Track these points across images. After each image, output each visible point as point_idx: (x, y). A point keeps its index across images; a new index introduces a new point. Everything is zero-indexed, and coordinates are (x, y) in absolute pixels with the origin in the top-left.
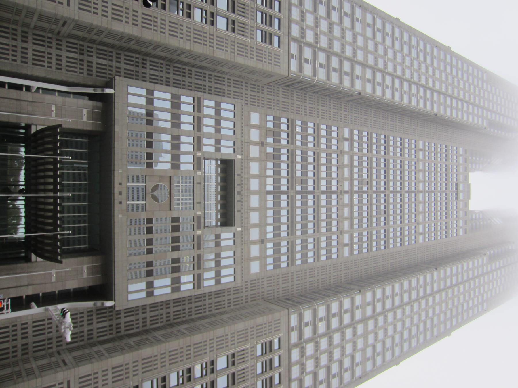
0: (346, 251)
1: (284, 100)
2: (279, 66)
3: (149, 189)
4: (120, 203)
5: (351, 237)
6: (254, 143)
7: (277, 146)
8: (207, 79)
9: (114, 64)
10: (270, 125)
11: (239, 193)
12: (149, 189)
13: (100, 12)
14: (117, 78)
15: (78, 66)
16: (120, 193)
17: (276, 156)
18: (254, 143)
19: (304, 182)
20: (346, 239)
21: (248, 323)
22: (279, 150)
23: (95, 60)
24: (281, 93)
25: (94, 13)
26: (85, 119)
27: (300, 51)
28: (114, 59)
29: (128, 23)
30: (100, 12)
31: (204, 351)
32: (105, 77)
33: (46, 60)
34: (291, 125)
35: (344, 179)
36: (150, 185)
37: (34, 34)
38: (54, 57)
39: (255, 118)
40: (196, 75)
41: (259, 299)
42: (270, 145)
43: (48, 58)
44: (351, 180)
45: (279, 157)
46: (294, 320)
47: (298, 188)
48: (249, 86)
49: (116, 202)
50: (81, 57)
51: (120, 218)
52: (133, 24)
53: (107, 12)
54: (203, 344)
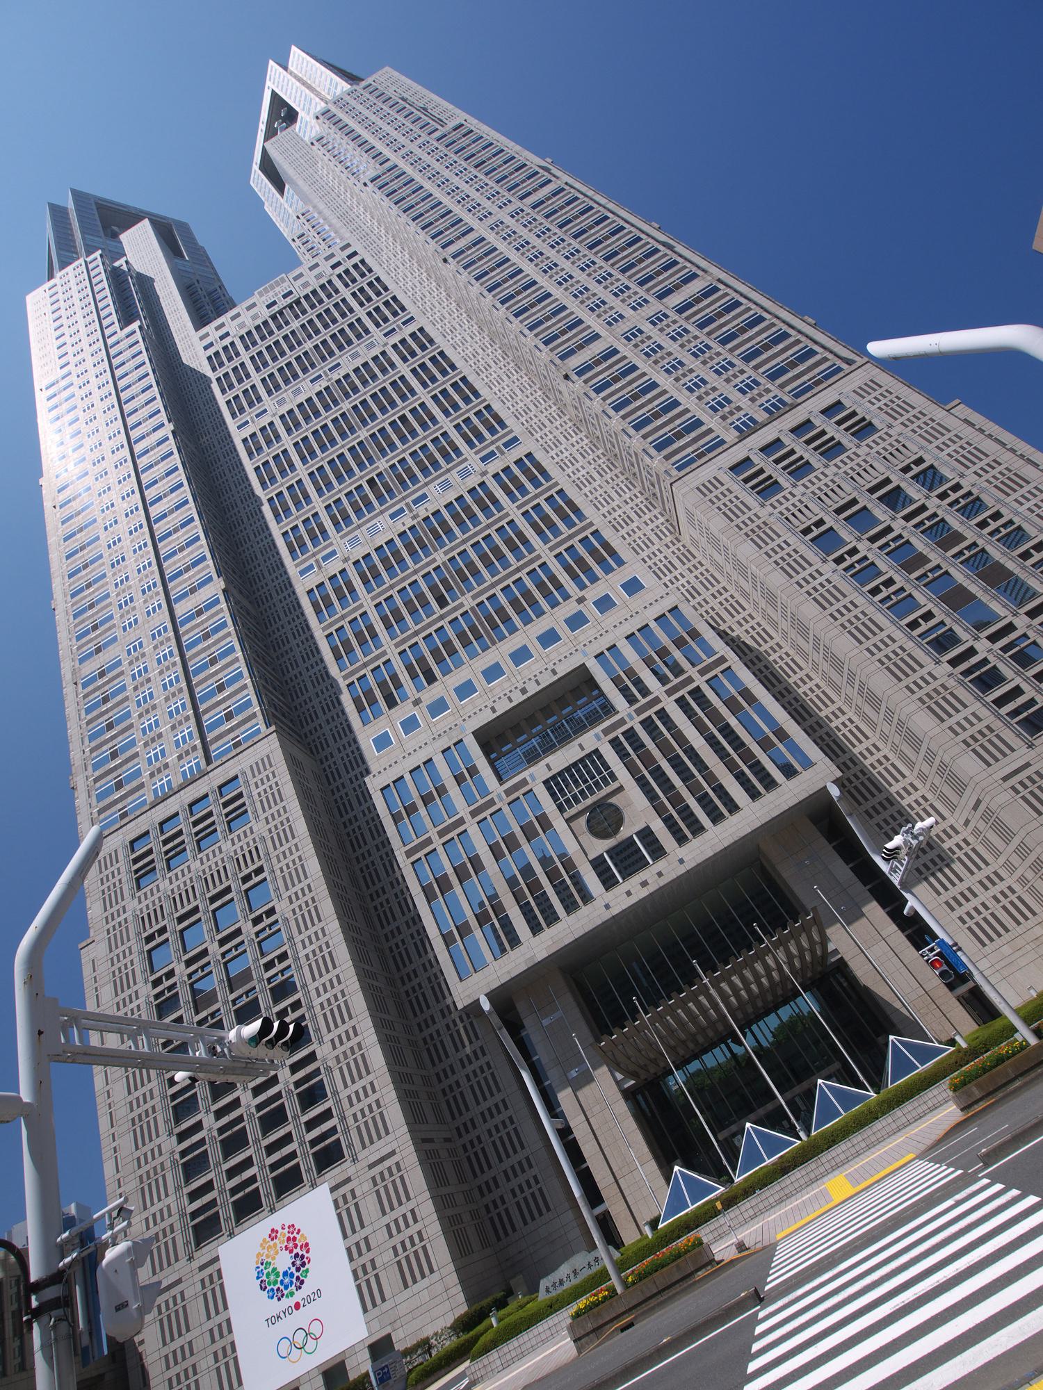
1: (331, 741)
2: (268, 756)
4: (660, 874)
8: (369, 860)
11: (524, 691)
13: (372, 1098)
14: (460, 1007)
15: (481, 1078)
16: (644, 884)
24: (312, 726)
25: (379, 1106)
26: (559, 1014)
28: (432, 1029)
29: (359, 1044)
30: (372, 1098)
31: (828, 586)
32: (471, 1024)
33: (503, 1133)
36: (599, 847)
37: (475, 1175)
38: (491, 1124)
40: (374, 884)
41: (684, 546)
43: (498, 1131)
48: (334, 785)
49: (663, 881)
50: (463, 1082)
52: (356, 1035)
53: (364, 1088)
54: (815, 595)
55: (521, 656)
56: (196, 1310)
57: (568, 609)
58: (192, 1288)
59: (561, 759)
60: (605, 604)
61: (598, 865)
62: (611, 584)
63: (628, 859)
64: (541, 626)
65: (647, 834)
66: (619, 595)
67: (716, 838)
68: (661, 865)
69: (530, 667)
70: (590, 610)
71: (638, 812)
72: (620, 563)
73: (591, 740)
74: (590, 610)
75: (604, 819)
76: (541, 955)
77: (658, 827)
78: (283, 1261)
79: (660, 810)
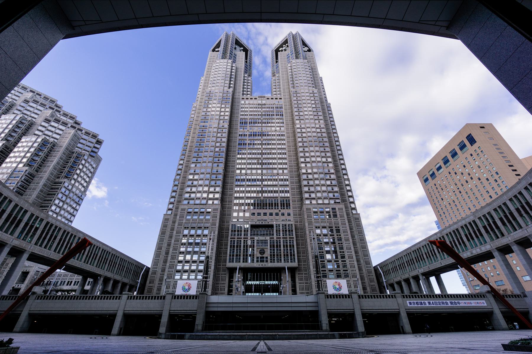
0: (285, 171)
3: (261, 256)
5: (280, 169)
6: (244, 214)
7: (245, 205)
9: (221, 267)
10: (237, 208)
12: (261, 256)
17: (248, 205)
18: (244, 214)
19: (258, 192)
20: (281, 171)
21: (306, 221)
22: (246, 204)
23: (221, 273)
27: (210, 199)
34: (236, 198)
35: (257, 173)
36: (259, 255)
39: (235, 214)
42: (245, 208)
44: (257, 169)
45: (249, 204)
46: (308, 202)
47: (260, 195)
51: (269, 265)
55: (265, 214)
56: (171, 287)
57: (277, 211)
58: (172, 284)
59: (262, 238)
60: (283, 214)
61: (258, 258)
62: (286, 211)
63: (262, 260)
64: (271, 211)
65: (267, 258)
66: (286, 214)
67: (276, 265)
68: (266, 264)
69: (265, 218)
70: (280, 214)
71: (267, 254)
72: (290, 208)
73: (268, 238)
74: (280, 214)
75: (262, 252)
76: (242, 266)
77: (269, 258)
78: (187, 287)
79: (271, 255)
